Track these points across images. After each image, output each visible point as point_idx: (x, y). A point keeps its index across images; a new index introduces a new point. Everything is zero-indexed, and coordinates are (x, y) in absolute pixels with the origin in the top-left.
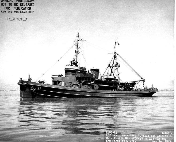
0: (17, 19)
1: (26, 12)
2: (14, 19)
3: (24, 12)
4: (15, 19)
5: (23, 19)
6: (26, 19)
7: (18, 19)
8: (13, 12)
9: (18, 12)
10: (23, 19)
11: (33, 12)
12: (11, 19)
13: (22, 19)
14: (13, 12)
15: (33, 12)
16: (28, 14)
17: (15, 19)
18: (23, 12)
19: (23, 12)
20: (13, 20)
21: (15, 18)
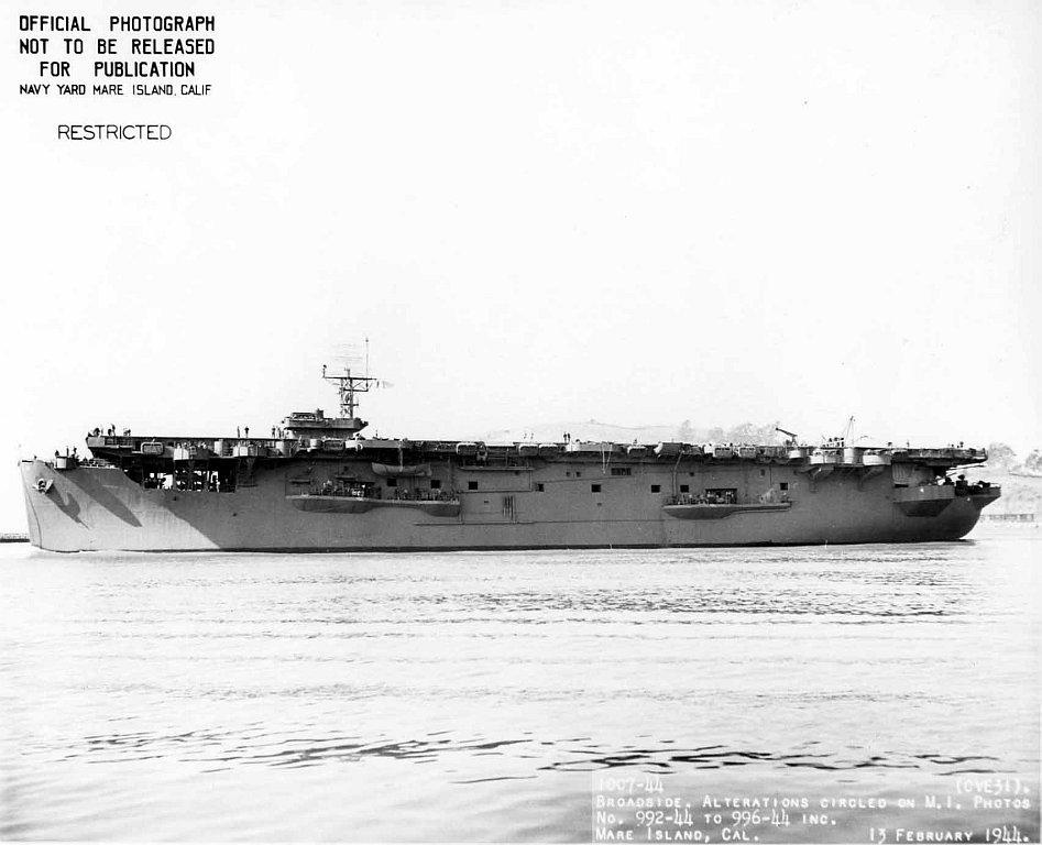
0: (113, 129)
1: (168, 90)
2: (96, 130)
3: (155, 91)
4: (104, 130)
5: (148, 131)
6: (165, 132)
7: (120, 132)
8: (89, 89)
9: (117, 89)
10: (148, 131)
11: (207, 88)
12: (81, 133)
13: (145, 130)
14: (89, 89)
15: (207, 88)
16: (177, 100)
17: (104, 130)
18: (149, 91)
19: (149, 91)
20: (91, 135)
21: (100, 126)
